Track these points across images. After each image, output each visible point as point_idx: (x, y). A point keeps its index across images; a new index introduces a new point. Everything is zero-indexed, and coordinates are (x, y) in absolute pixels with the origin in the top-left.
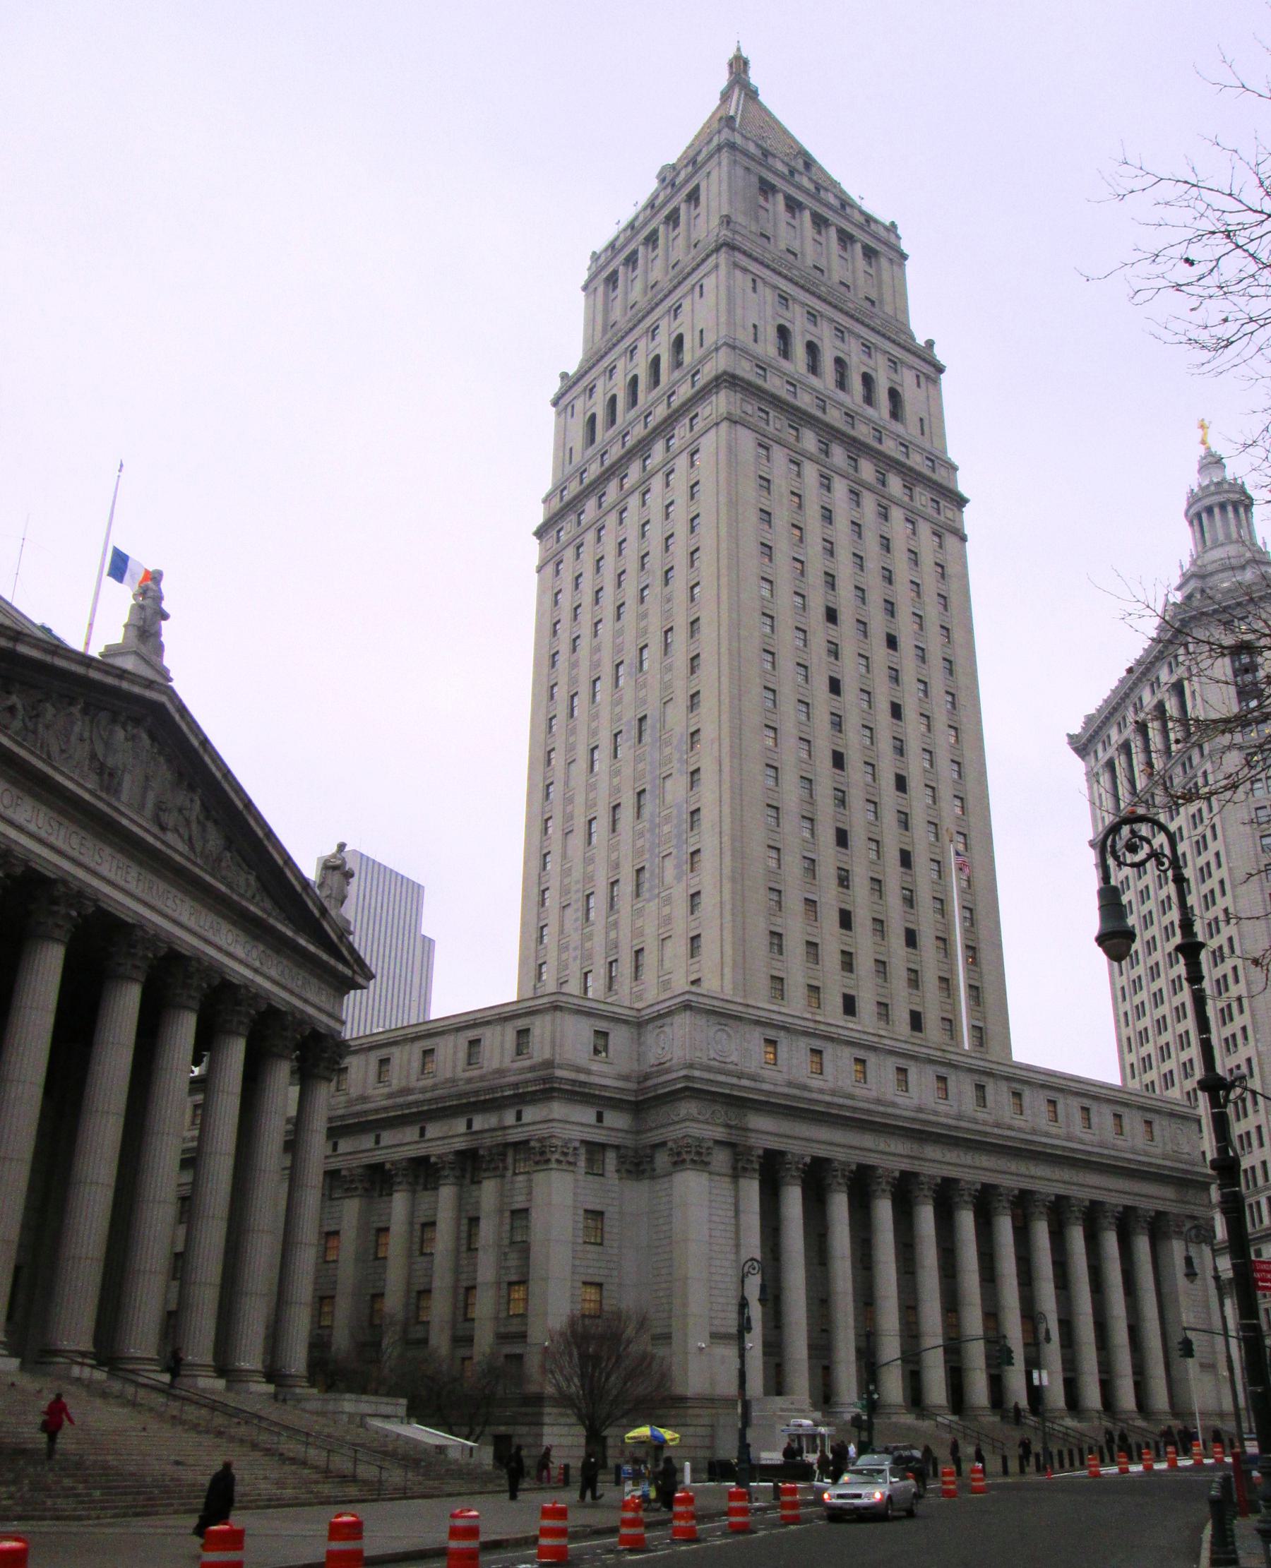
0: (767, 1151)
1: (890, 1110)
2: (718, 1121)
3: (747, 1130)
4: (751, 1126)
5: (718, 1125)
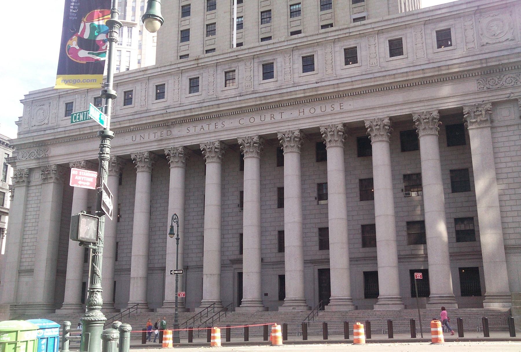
3: (48, 157)
4: (50, 155)
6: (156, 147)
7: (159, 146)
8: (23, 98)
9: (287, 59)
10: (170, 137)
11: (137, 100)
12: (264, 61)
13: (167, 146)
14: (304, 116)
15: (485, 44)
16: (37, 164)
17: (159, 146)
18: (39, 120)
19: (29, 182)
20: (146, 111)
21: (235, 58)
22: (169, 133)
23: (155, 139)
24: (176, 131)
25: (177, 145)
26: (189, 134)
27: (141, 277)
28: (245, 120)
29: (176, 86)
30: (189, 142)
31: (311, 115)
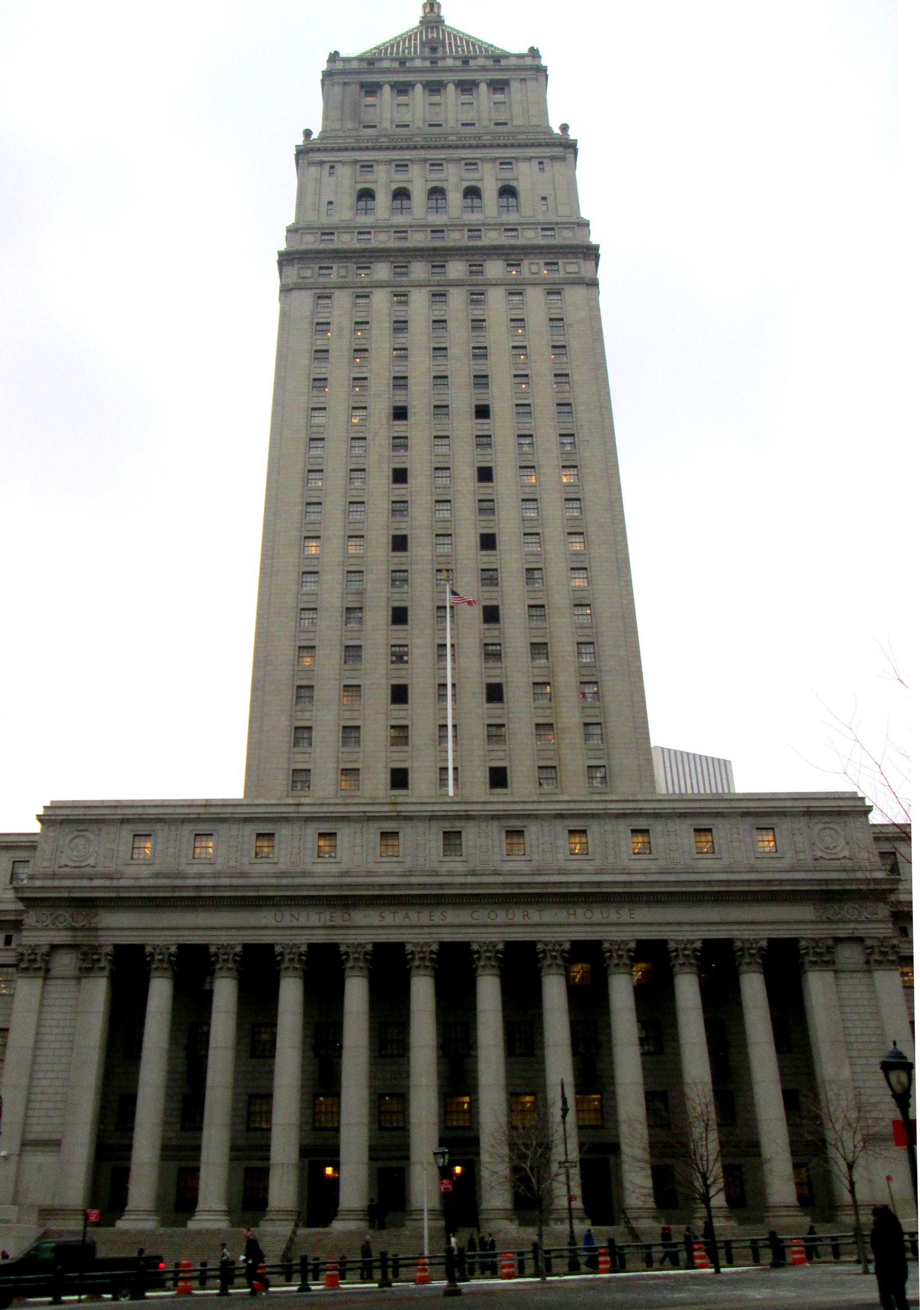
0: (117, 947)
1: (299, 881)
2: (61, 926)
3: (96, 929)
4: (101, 925)
5: (60, 929)
6: (323, 937)
8: (41, 812)
9: (546, 830)
10: (347, 923)
13: (345, 938)
14: (576, 921)
15: (818, 857)
16: (69, 939)
18: (76, 856)
19: (48, 970)
20: (305, 874)
21: (464, 813)
22: (346, 917)
24: (360, 917)
25: (362, 939)
26: (383, 923)
28: (482, 915)
29: (358, 841)
30: (383, 937)
31: (587, 921)
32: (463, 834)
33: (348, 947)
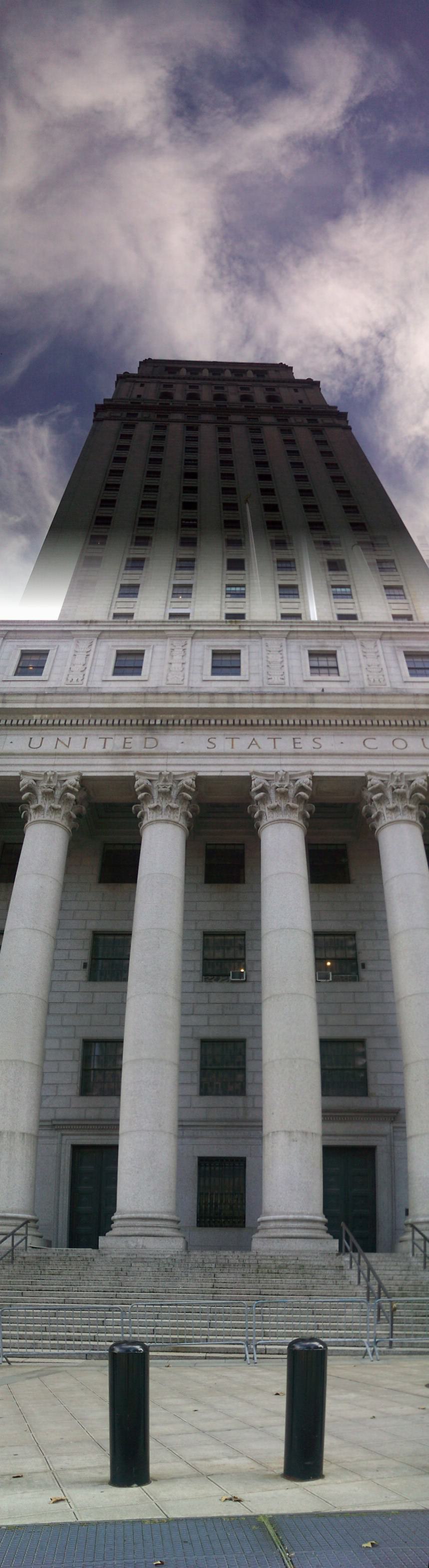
7: (116, 769)
10: (153, 750)
11: (57, 670)
12: (407, 647)
17: (116, 769)
22: (151, 743)
23: (104, 750)
24: (171, 741)
27: (23, 1134)
28: (381, 742)
32: (339, 655)
33: (150, 781)
